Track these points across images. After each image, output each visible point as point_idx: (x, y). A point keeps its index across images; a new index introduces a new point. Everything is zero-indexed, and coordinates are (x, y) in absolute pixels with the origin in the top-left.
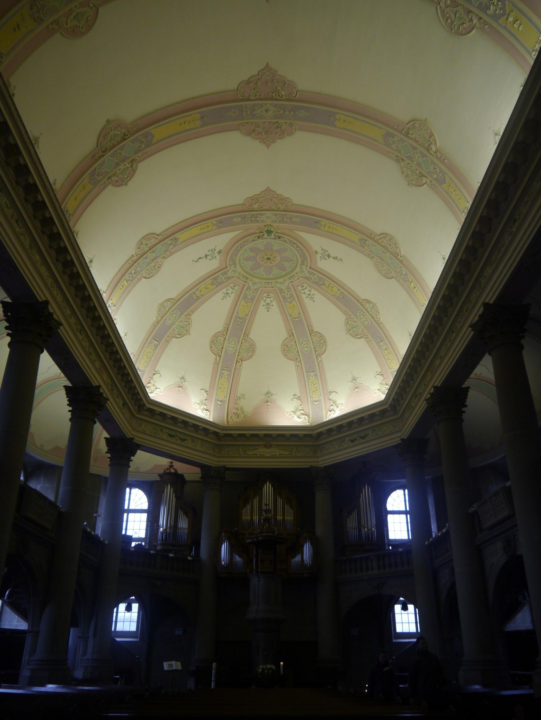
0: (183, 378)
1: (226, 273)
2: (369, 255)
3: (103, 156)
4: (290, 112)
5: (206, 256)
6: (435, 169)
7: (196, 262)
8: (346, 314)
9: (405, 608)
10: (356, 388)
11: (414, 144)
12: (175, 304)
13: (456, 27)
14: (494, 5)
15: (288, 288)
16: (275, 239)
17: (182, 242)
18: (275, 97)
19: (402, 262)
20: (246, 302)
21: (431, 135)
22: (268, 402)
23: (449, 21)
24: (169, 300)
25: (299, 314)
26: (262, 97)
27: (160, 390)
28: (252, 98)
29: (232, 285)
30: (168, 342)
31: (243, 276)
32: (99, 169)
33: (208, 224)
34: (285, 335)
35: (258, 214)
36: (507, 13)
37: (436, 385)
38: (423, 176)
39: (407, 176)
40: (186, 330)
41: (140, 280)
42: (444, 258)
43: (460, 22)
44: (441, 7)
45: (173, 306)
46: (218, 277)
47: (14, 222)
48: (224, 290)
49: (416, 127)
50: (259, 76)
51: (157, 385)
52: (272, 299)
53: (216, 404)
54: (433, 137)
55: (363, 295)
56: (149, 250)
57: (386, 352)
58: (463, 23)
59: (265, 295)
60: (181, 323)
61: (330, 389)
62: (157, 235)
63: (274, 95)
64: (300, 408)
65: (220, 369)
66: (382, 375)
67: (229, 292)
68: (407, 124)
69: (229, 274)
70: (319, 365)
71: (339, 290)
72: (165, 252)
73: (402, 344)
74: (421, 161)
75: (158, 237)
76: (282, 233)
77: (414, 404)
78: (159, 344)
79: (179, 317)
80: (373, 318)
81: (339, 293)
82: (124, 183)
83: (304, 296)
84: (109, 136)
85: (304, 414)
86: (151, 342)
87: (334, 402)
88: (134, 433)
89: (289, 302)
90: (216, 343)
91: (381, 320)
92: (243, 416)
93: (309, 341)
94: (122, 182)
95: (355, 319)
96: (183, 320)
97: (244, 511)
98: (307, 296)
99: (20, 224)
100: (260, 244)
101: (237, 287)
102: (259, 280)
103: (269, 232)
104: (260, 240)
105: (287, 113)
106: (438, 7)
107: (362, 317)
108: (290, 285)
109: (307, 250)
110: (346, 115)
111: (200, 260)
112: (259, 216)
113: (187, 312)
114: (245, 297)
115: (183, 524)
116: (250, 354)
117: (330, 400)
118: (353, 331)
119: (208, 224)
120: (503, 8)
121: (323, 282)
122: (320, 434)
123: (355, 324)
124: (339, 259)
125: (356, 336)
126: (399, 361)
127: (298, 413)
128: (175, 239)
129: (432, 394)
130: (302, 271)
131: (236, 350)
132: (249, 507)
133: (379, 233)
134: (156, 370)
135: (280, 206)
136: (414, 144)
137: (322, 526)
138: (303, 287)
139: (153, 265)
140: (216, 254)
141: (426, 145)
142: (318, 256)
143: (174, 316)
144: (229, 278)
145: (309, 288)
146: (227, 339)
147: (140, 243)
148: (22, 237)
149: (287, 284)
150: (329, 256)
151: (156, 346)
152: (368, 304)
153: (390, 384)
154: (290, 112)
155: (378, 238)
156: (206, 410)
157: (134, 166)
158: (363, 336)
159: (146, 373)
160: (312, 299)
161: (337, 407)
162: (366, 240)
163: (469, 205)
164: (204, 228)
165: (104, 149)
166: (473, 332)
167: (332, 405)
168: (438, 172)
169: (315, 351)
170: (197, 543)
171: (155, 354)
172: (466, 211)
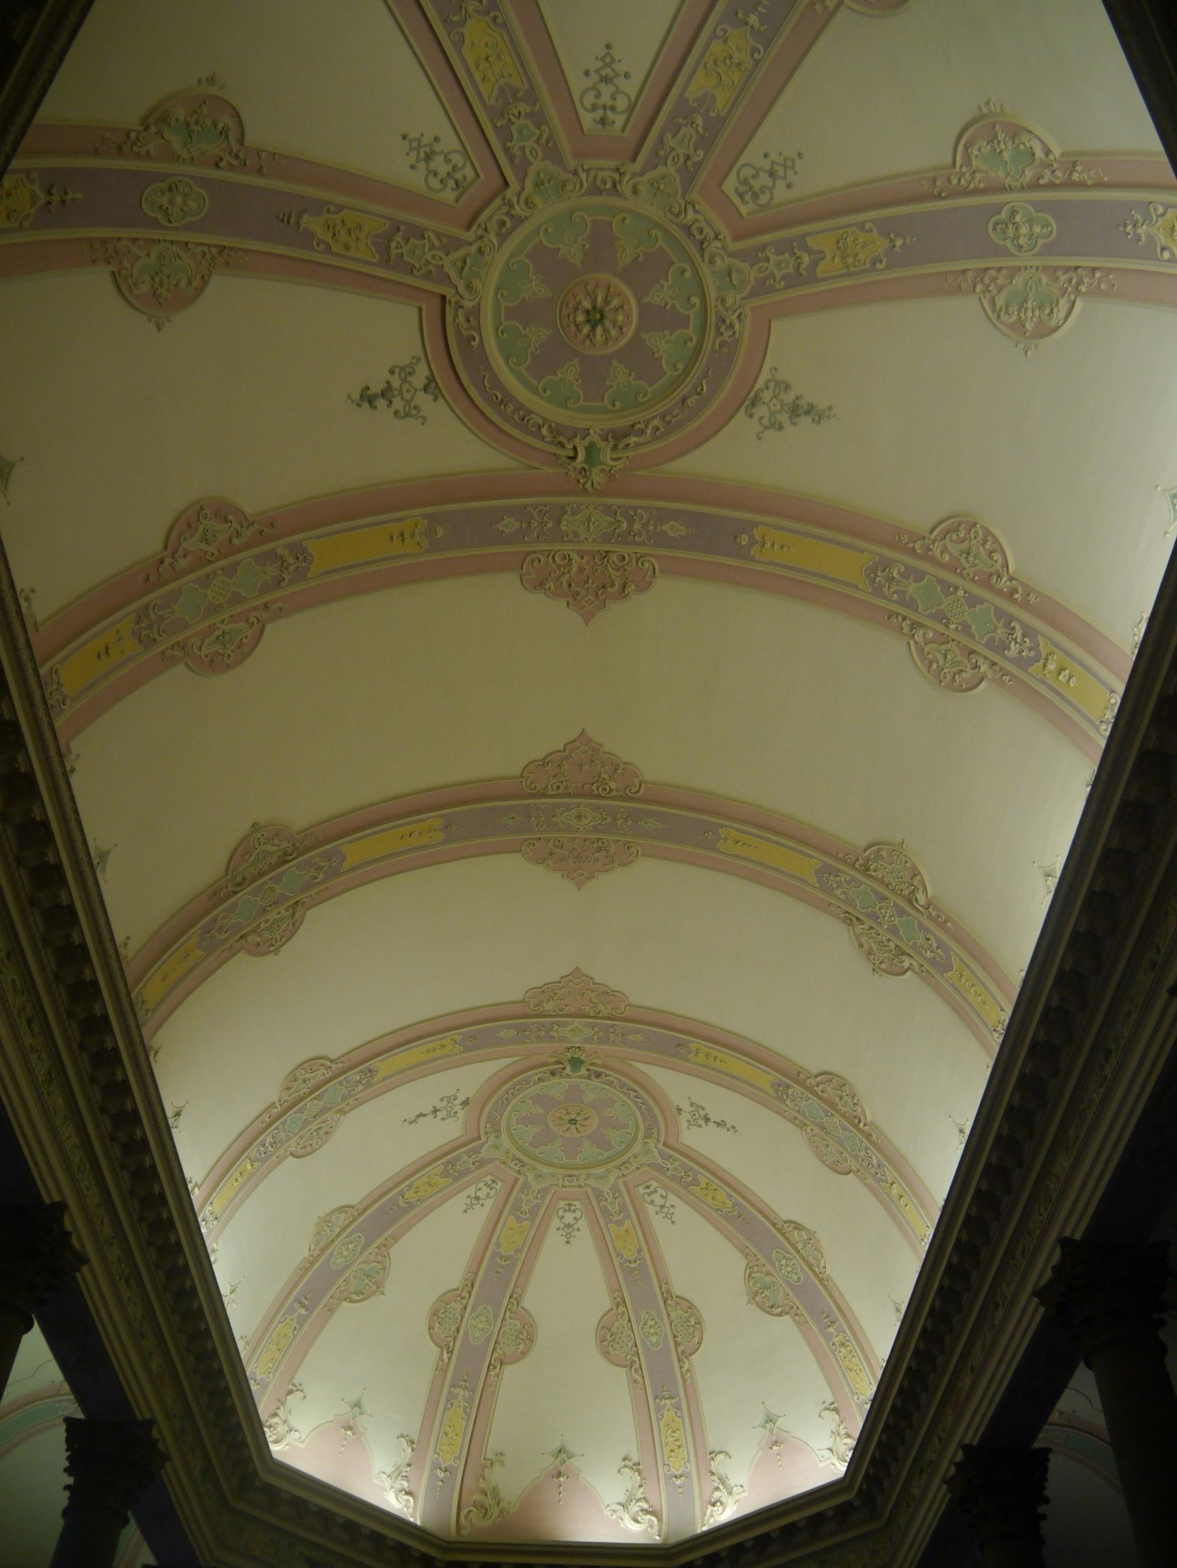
0: (358, 1405)
1: (476, 1151)
2: (795, 1118)
3: (235, 893)
4: (626, 820)
5: (435, 1111)
6: (928, 939)
7: (411, 1123)
8: (747, 1256)
10: (776, 1443)
11: (881, 889)
12: (355, 1219)
13: (948, 676)
14: (1016, 643)
15: (615, 1189)
16: (589, 1077)
17: (385, 1079)
19: (868, 1136)
20: (519, 1220)
21: (915, 873)
22: (559, 1474)
23: (934, 666)
24: (341, 1209)
25: (640, 1250)
26: (571, 791)
27: (302, 1438)
29: (488, 1179)
30: (331, 1310)
31: (515, 1158)
33: (444, 1042)
34: (606, 1303)
35: (553, 1023)
36: (1043, 656)
37: (967, 1441)
38: (904, 953)
39: (870, 954)
40: (376, 1283)
41: (280, 1160)
42: (961, 1131)
44: (916, 643)
45: (351, 1223)
46: (458, 1158)
47: (24, 1024)
48: (471, 1191)
51: (294, 1421)
52: (578, 1214)
53: (433, 1477)
54: (918, 878)
55: (786, 1210)
56: (311, 1093)
57: (843, 1350)
58: (962, 671)
59: (562, 1204)
60: (366, 1267)
61: (713, 1443)
62: (332, 1061)
63: (594, 787)
64: (639, 1495)
65: (448, 1382)
66: (836, 1410)
67: (482, 1194)
68: (865, 850)
69: (484, 1153)
70: (684, 1380)
71: (730, 1196)
72: (344, 1098)
73: (881, 1333)
74: (896, 922)
75: (334, 1066)
76: (604, 1066)
78: (308, 1317)
79: (363, 1249)
80: (810, 1266)
81: (729, 1204)
83: (651, 1210)
85: (645, 1511)
86: (290, 1311)
87: (722, 1480)
89: (616, 1223)
90: (444, 1318)
91: (828, 1271)
92: (496, 1512)
93: (660, 1317)
94: (268, 947)
95: (769, 1267)
96: (372, 1258)
98: (658, 1209)
99: (36, 1028)
100: (557, 1087)
101: (500, 1184)
102: (551, 1170)
103: (576, 1063)
104: (556, 1080)
107: (783, 1262)
108: (620, 1182)
109: (660, 1106)
110: (737, 830)
111: (421, 1119)
112: (555, 1027)
113: (381, 1240)
114: (517, 1208)
116: (521, 1347)
117: (712, 1473)
118: (765, 1299)
119: (444, 1042)
120: (1035, 647)
121: (694, 1177)
123: (769, 1279)
124: (729, 1126)
125: (770, 1309)
126: (874, 1374)
127: (635, 1508)
128: (370, 1071)
129: (959, 1466)
130: (648, 1152)
131: (488, 1339)
133: (815, 1071)
134: (296, 1380)
135: (602, 1008)
136: (881, 889)
138: (648, 1187)
139: (314, 1126)
140: (458, 1108)
141: (906, 892)
142: (684, 1117)
143: (351, 1246)
144: (482, 1163)
145: (661, 1191)
146: (469, 1308)
147: (293, 1077)
148: (33, 1057)
149: (612, 1179)
150: (707, 1120)
151: (302, 1321)
152: (796, 1232)
153: (857, 1435)
154: (626, 820)
155: (813, 1081)
156: (409, 1493)
157: (297, 915)
158: (787, 1309)
159: (271, 1387)
160: (669, 1216)
161: (730, 1493)
162: (788, 1087)
163: (1006, 1017)
164: (434, 1049)
165: (239, 879)
166: (1042, 1310)
167: (717, 1489)
168: (934, 946)
169: (677, 1344)
171: (298, 1339)
172: (1002, 1029)
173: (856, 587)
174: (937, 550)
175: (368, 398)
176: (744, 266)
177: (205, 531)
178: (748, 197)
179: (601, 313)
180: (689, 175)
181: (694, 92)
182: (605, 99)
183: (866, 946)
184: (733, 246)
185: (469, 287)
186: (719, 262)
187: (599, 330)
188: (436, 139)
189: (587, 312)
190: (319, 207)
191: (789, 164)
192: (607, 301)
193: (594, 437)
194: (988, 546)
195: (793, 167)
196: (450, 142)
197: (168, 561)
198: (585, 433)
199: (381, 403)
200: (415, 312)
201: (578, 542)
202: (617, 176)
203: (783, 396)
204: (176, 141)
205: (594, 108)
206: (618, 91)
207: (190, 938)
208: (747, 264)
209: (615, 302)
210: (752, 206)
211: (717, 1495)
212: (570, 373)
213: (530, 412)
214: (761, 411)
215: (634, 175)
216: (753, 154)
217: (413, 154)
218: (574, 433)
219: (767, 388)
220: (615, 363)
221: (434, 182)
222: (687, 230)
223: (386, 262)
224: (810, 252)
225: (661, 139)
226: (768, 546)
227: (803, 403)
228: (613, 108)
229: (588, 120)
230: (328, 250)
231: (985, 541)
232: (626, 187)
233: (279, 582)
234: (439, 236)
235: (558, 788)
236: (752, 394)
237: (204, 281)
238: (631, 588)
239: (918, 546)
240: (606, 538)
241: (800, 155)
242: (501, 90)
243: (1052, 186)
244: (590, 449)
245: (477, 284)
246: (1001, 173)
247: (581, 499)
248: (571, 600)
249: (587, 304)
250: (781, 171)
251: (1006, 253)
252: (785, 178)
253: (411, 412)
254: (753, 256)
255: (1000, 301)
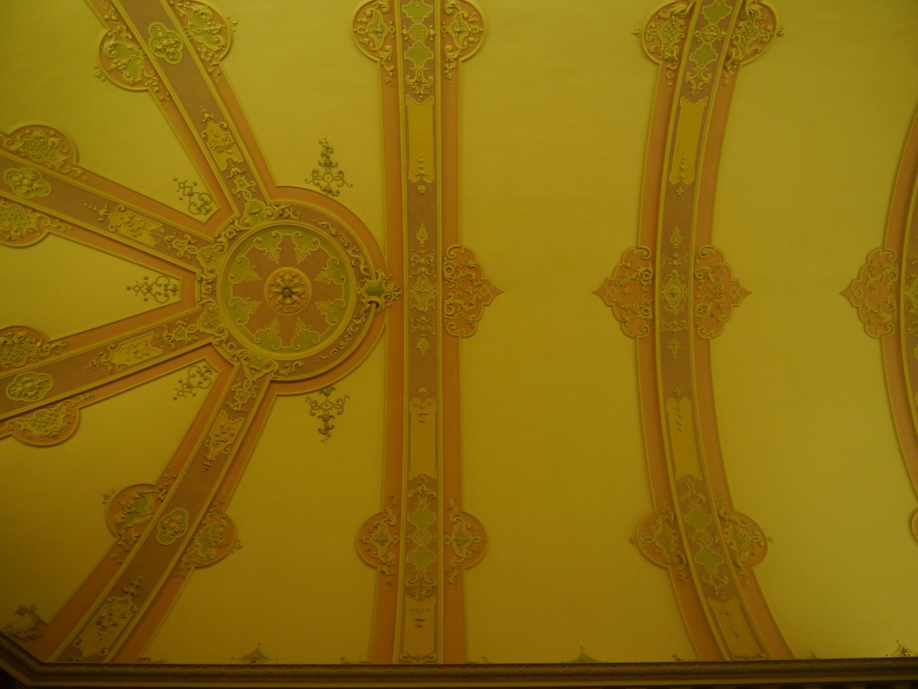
3: (688, 565)
4: (674, 258)
13: (474, 27)
18: (650, 282)
21: (657, 17)
23: (471, 39)
26: (649, 302)
28: (650, 317)
32: (707, 578)
35: (907, 314)
39: (762, 42)
43: (466, 23)
44: (460, 56)
49: (656, 48)
50: (614, 305)
58: (464, 18)
63: (646, 283)
68: (657, 64)
74: (715, 24)
82: (762, 544)
84: (658, 544)
94: (759, 546)
105: (676, 263)
106: (461, 59)
141: (682, 22)
154: (674, 258)
157: (734, 518)
165: (676, 560)
173: (434, 107)
174: (384, 55)
175: (326, 431)
176: (247, 206)
177: (377, 541)
178: (208, 207)
179: (285, 289)
180: (199, 242)
181: (151, 242)
182: (161, 290)
183: (755, 47)
184: (237, 213)
185: (268, 366)
186: (246, 221)
187: (294, 290)
188: (180, 382)
189: (285, 297)
190: (204, 449)
191: (182, 186)
192: (278, 286)
193: (362, 291)
194: (365, 20)
195: (184, 183)
196: (183, 375)
197: (385, 569)
198: (360, 296)
199: (331, 422)
200: (280, 399)
201: (436, 299)
202: (204, 282)
203: (321, 174)
204: (137, 520)
205: (166, 296)
206: (156, 283)
207: (710, 608)
208: (246, 204)
209: (279, 281)
210: (212, 205)
212: (323, 306)
213: (345, 331)
214: (334, 186)
215: (203, 272)
216: (182, 207)
217: (186, 394)
218: (359, 303)
219: (318, 184)
220: (316, 279)
221: (206, 384)
222: (231, 241)
223: (245, 414)
224: (229, 168)
225: (182, 258)
226: (422, 172)
227: (323, 160)
228: (166, 286)
229: (174, 299)
230: (231, 445)
231: (362, 23)
232: (210, 277)
233: (433, 499)
234: (234, 382)
235: (646, 311)
236: (324, 193)
237: (226, 518)
238: (471, 263)
239: (389, 69)
240: (433, 281)
241: (175, 180)
242: (154, 346)
243: (128, 30)
244: (370, 293)
245: (265, 362)
246: (139, 62)
247: (406, 298)
248: (483, 304)
249: (280, 297)
250: (188, 190)
251: (185, 49)
252: (191, 187)
253: (340, 406)
254: (240, 200)
255: (215, 48)
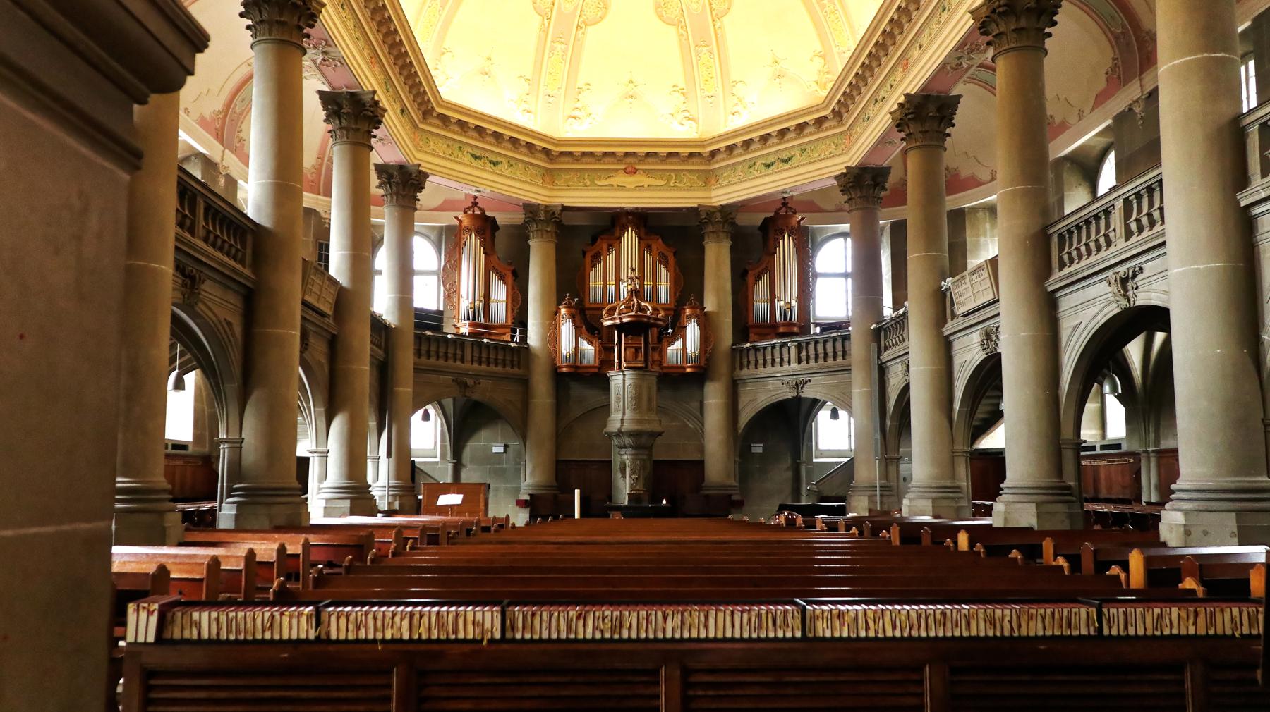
9: (835, 415)
37: (908, 91)
61: (735, 76)
77: (871, 114)
88: (419, 155)
97: (592, 274)
115: (500, 292)
122: (713, 154)
129: (901, 105)
131: (576, 9)
132: (600, 266)
137: (716, 297)
170: (520, 321)
211: (736, 109)
